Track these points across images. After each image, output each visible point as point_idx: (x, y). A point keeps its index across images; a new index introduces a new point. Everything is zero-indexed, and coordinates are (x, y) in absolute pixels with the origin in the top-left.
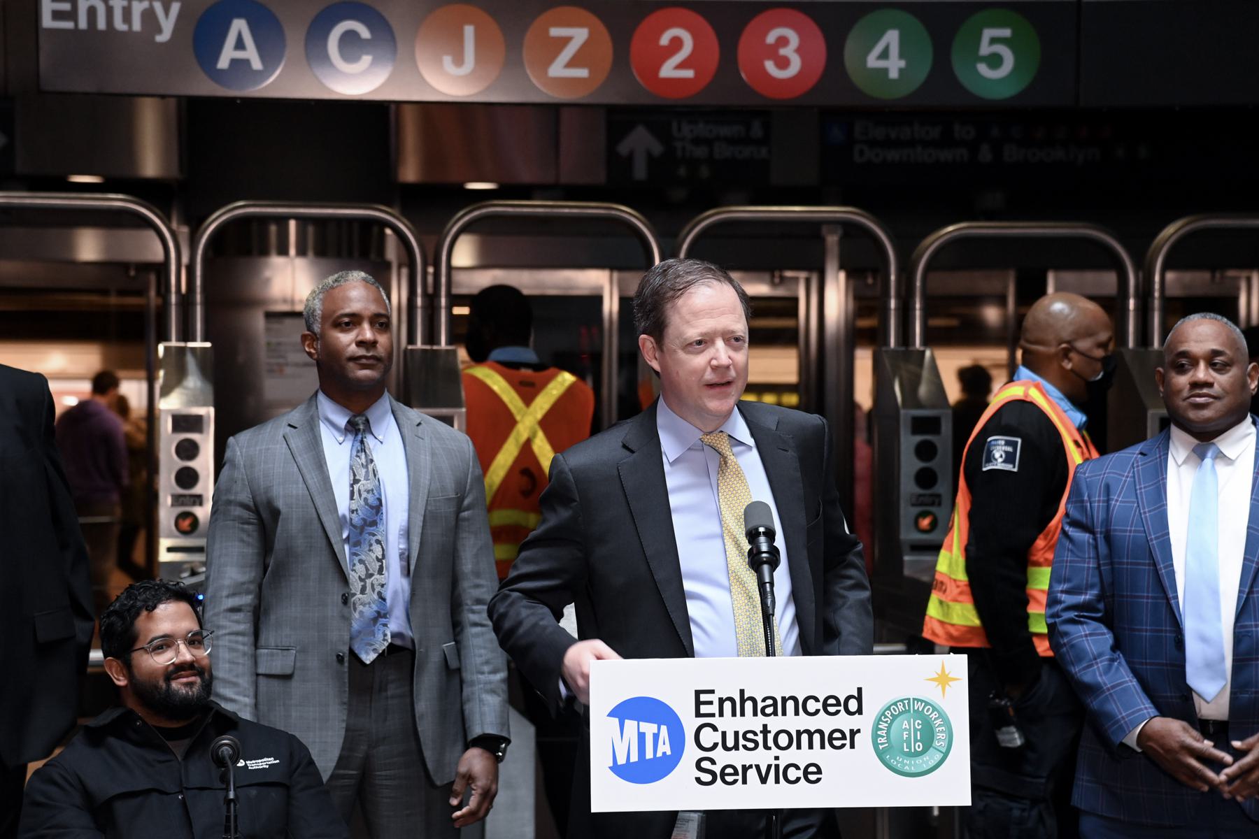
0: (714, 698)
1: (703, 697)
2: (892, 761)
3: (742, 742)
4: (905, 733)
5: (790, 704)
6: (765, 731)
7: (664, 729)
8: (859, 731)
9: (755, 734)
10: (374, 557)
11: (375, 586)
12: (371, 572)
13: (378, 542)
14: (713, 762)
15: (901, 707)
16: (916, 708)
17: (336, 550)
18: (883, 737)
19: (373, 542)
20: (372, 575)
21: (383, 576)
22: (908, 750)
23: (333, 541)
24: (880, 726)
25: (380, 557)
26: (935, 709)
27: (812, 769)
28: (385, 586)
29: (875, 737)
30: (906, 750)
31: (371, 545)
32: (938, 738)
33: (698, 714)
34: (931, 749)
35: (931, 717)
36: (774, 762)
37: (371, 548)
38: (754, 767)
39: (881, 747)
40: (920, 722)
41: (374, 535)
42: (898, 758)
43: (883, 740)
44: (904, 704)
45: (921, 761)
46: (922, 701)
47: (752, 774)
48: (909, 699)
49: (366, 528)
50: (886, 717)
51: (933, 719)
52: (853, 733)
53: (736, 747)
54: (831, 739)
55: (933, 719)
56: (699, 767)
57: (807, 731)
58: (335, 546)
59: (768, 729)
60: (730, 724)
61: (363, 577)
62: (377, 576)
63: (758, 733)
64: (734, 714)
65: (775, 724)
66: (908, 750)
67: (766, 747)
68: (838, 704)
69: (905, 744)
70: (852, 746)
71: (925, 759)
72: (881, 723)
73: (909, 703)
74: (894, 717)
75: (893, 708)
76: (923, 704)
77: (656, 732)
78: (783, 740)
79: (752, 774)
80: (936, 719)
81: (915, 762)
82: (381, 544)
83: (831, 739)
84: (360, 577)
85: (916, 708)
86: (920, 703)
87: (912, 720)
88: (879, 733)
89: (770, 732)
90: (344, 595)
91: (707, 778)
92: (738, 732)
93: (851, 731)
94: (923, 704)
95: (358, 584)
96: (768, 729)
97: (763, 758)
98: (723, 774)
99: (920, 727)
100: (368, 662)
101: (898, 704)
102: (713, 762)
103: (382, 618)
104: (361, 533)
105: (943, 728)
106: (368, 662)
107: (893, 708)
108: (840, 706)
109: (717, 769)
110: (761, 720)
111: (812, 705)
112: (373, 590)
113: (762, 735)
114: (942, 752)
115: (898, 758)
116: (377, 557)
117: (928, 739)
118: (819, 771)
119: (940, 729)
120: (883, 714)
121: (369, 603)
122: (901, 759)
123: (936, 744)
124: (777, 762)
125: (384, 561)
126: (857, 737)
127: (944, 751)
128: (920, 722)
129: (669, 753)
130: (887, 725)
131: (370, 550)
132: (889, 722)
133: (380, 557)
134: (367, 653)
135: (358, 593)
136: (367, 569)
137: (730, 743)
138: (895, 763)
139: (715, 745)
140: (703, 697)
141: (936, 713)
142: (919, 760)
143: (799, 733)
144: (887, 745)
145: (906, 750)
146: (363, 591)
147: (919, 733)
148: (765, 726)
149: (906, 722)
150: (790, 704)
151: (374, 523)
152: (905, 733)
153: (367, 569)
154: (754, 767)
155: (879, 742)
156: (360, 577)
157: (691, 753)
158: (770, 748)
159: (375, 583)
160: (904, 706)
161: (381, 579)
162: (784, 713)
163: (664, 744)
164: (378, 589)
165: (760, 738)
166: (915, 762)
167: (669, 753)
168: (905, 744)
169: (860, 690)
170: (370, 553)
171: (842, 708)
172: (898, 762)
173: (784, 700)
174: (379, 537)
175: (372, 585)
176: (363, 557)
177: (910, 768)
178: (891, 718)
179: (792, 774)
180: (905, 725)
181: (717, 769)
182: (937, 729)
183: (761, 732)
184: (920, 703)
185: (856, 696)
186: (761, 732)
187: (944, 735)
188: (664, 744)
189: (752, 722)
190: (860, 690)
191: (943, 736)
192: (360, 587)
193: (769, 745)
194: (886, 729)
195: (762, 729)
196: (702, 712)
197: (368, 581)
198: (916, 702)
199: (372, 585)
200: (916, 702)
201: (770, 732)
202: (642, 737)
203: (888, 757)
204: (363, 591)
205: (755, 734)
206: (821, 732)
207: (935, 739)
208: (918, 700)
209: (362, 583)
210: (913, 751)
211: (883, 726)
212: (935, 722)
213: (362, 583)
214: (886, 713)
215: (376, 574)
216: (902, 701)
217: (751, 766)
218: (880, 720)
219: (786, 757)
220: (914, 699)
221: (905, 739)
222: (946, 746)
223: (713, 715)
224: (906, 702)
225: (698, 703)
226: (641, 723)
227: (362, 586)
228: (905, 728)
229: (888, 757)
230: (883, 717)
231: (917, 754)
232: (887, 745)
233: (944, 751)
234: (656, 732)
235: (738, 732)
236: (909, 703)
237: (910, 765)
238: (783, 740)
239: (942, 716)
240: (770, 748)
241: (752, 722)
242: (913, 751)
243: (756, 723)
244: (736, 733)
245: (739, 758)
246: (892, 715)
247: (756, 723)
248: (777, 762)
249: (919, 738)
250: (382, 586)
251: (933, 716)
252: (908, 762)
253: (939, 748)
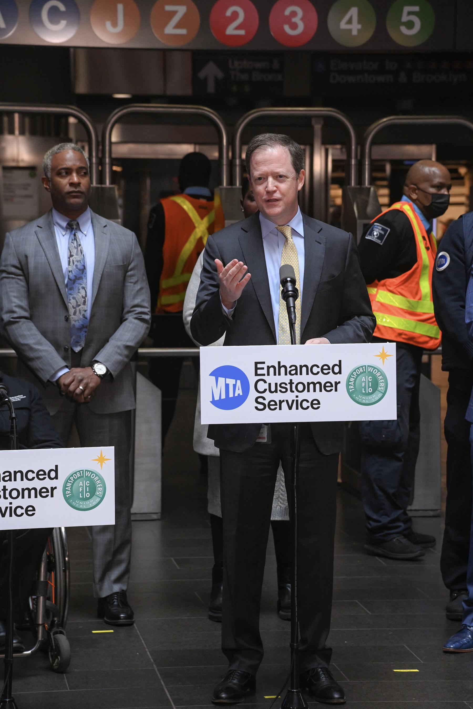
0: (265, 366)
1: (259, 366)
2: (356, 397)
3: (279, 388)
4: (363, 383)
6: (291, 383)
7: (239, 382)
8: (339, 382)
10: (81, 295)
11: (81, 311)
12: (79, 303)
13: (83, 288)
14: (264, 399)
16: (369, 371)
17: (62, 293)
18: (352, 385)
19: (80, 288)
20: (79, 305)
21: (85, 306)
22: (365, 392)
23: (60, 287)
24: (350, 380)
25: (84, 296)
26: (379, 371)
28: (87, 311)
29: (348, 385)
30: (363, 392)
31: (79, 290)
32: (380, 385)
34: (377, 391)
35: (376, 375)
36: (296, 399)
37: (79, 291)
38: (285, 401)
39: (351, 391)
40: (371, 378)
41: (81, 284)
42: (359, 396)
43: (352, 387)
45: (371, 397)
46: (372, 367)
47: (284, 405)
48: (365, 366)
49: (77, 280)
51: (378, 376)
52: (337, 383)
53: (276, 391)
54: (325, 386)
55: (378, 376)
56: (257, 401)
58: (61, 291)
59: (293, 382)
60: (272, 379)
61: (75, 306)
62: (82, 306)
63: (288, 384)
64: (275, 374)
65: (296, 379)
66: (365, 392)
67: (292, 391)
68: (329, 369)
69: (363, 389)
71: (373, 396)
72: (351, 378)
73: (365, 368)
75: (357, 371)
76: (373, 368)
77: (235, 383)
78: (300, 387)
79: (284, 405)
80: (379, 376)
81: (368, 398)
82: (85, 289)
83: (325, 386)
84: (73, 306)
85: (369, 371)
87: (367, 376)
88: (350, 383)
89: (293, 383)
90: (66, 316)
91: (261, 407)
92: (277, 383)
93: (336, 383)
94: (373, 368)
95: (72, 310)
96: (293, 382)
97: (290, 396)
98: (269, 405)
99: (371, 380)
100: (77, 351)
101: (360, 368)
102: (264, 399)
103: (84, 328)
104: (74, 283)
105: (383, 380)
106: (77, 351)
107: (357, 371)
109: (266, 402)
110: (289, 377)
111: (315, 370)
112: (80, 313)
113: (289, 385)
114: (382, 393)
116: (82, 296)
118: (319, 403)
119: (381, 381)
120: (352, 374)
121: (78, 320)
123: (379, 389)
124: (297, 399)
125: (86, 298)
126: (339, 385)
127: (383, 392)
128: (371, 378)
129: (241, 394)
130: (354, 379)
131: (79, 292)
132: (355, 378)
133: (84, 296)
134: (76, 346)
135: (72, 315)
136: (77, 302)
137: (273, 389)
138: (358, 399)
140: (259, 366)
141: (379, 373)
143: (309, 384)
144: (354, 389)
146: (75, 313)
147: (370, 383)
148: (291, 380)
150: (304, 369)
151: (80, 278)
153: (77, 302)
154: (285, 401)
155: (350, 388)
156: (73, 306)
157: (253, 394)
158: (293, 392)
159: (81, 309)
160: (363, 369)
161: (85, 307)
162: (301, 374)
163: (239, 390)
164: (83, 312)
165: (288, 387)
166: (368, 398)
167: (241, 394)
168: (363, 389)
169: (340, 361)
170: (79, 294)
171: (331, 371)
172: (359, 398)
173: (301, 367)
174: (84, 286)
175: (80, 310)
176: (75, 296)
178: (356, 376)
179: (305, 404)
180: (363, 379)
181: (266, 402)
182: (380, 381)
183: (289, 383)
185: (338, 365)
186: (289, 383)
188: (239, 390)
189: (284, 378)
190: (340, 361)
191: (383, 385)
192: (73, 311)
193: (293, 390)
194: (353, 381)
195: (289, 382)
196: (258, 373)
197: (78, 309)
198: (369, 367)
199: (80, 310)
200: (369, 367)
201: (293, 383)
202: (227, 386)
203: (354, 395)
204: (75, 313)
205: (286, 384)
206: (320, 383)
207: (379, 386)
208: (370, 366)
209: (75, 310)
210: (367, 392)
211: (352, 380)
212: (379, 378)
213: (75, 310)
214: (354, 373)
215: (82, 305)
216: (362, 367)
217: (283, 401)
219: (302, 396)
221: (363, 386)
222: (384, 390)
223: (264, 375)
224: (364, 367)
225: (257, 369)
226: (227, 379)
227: (74, 311)
229: (354, 395)
231: (369, 394)
232: (354, 389)
233: (383, 392)
234: (235, 383)
235: (277, 383)
236: (365, 368)
237: (365, 400)
238: (300, 387)
240: (293, 392)
241: (284, 378)
242: (367, 392)
243: (287, 379)
244: (276, 384)
245: (278, 397)
246: (357, 374)
247: (287, 379)
248: (297, 399)
249: (370, 386)
250: (85, 311)
251: (378, 374)
252: (365, 398)
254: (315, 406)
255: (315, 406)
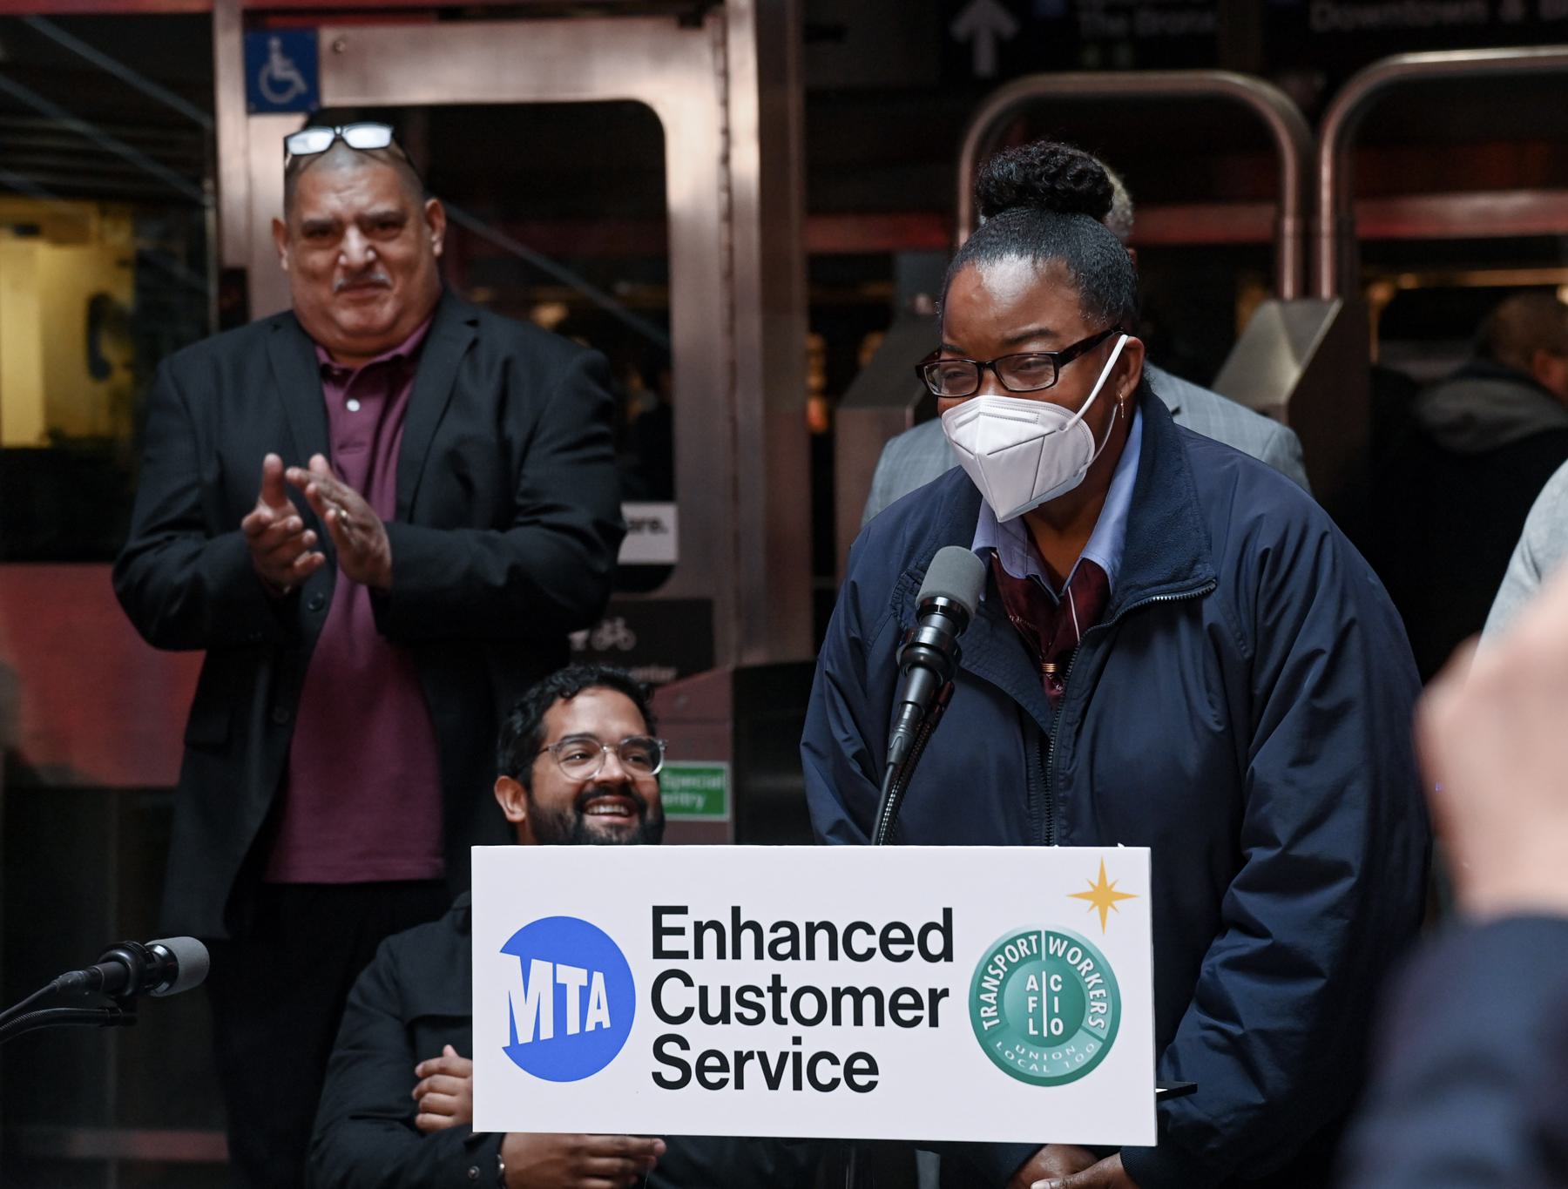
1: (668, 921)
3: (735, 1007)
4: (1031, 999)
5: (822, 937)
6: (777, 988)
9: (759, 993)
15: (1024, 949)
16: (1051, 951)
18: (990, 1005)
22: (1036, 1033)
24: (984, 985)
26: (1087, 954)
27: (861, 1064)
29: (976, 1004)
30: (1032, 1032)
32: (1093, 1010)
33: (659, 953)
38: (756, 1055)
39: (986, 1025)
40: (1060, 979)
42: (1018, 1047)
43: (991, 1012)
44: (1029, 942)
45: (1060, 1055)
46: (1063, 938)
47: (753, 1069)
48: (1038, 933)
50: (996, 967)
51: (1083, 973)
52: (936, 996)
53: (725, 1017)
57: (851, 991)
59: (783, 985)
60: (713, 972)
63: (765, 990)
64: (721, 955)
66: (1036, 1033)
69: (1031, 1021)
70: (934, 1022)
73: (1038, 941)
74: (1012, 968)
75: (1010, 951)
76: (1066, 943)
78: (809, 1006)
79: (753, 1069)
80: (1089, 973)
85: (1051, 951)
86: (1058, 941)
87: (1044, 973)
88: (983, 997)
91: (673, 1074)
96: (783, 985)
98: (702, 1068)
99: (1060, 987)
101: (1019, 942)
102: (684, 1045)
105: (1103, 991)
107: (1010, 951)
108: (912, 943)
109: (691, 1058)
110: (769, 966)
111: (861, 942)
113: (771, 994)
115: (1018, 1047)
117: (1074, 1010)
118: (873, 1069)
119: (1097, 993)
120: (991, 961)
122: (1023, 1050)
123: (1090, 1022)
124: (797, 1048)
126: (943, 1003)
128: (1060, 979)
130: (997, 983)
132: (1001, 977)
137: (715, 1009)
138: (1013, 1057)
139: (688, 1013)
140: (668, 921)
141: (1088, 961)
142: (1057, 1054)
143: (837, 994)
144: (997, 1021)
145: (1032, 1032)
147: (1056, 999)
149: (1032, 978)
150: (822, 937)
152: (1031, 999)
154: (756, 1055)
155: (983, 1015)
158: (783, 1022)
160: (1029, 947)
162: (811, 955)
165: (767, 1002)
168: (1031, 1021)
169: (948, 913)
171: (915, 947)
172: (1017, 1055)
173: (811, 929)
177: (1041, 1068)
178: (1006, 969)
179: (825, 1072)
181: (691, 1058)
182: (1092, 993)
183: (769, 989)
184: (1058, 941)
185: (941, 923)
186: (769, 989)
187: (1105, 1005)
189: (753, 971)
190: (948, 913)
191: (1102, 1008)
193: (784, 1015)
194: (996, 990)
198: (1051, 939)
200: (1051, 939)
205: (759, 993)
208: (1056, 935)
210: (1045, 1035)
211: (990, 984)
212: (1087, 980)
214: (996, 959)
218: (985, 972)
220: (1048, 934)
221: (1030, 1010)
223: (683, 955)
225: (659, 932)
228: (1032, 990)
230: (990, 967)
231: (1054, 1042)
232: (997, 1021)
236: (1038, 941)
237: (1040, 1063)
238: (809, 1006)
239: (1101, 967)
240: (783, 1022)
241: (753, 971)
242: (1045, 1035)
243: (759, 972)
244: (725, 991)
245: (730, 1038)
246: (1007, 963)
247: (759, 972)
248: (797, 1048)
249: (1056, 1010)
251: (1085, 967)
252: (1036, 1057)
253: (1095, 1031)
254: (861, 1080)
255: (861, 1080)
